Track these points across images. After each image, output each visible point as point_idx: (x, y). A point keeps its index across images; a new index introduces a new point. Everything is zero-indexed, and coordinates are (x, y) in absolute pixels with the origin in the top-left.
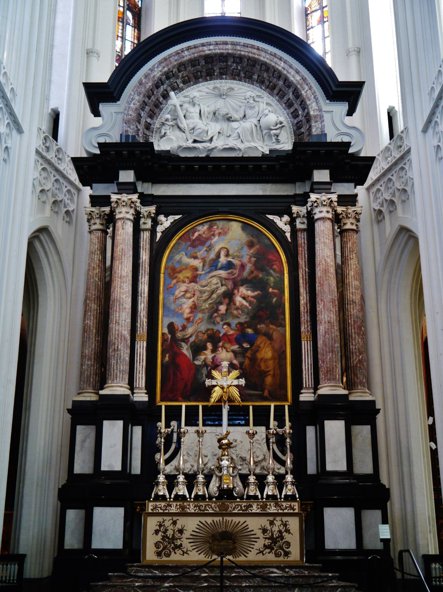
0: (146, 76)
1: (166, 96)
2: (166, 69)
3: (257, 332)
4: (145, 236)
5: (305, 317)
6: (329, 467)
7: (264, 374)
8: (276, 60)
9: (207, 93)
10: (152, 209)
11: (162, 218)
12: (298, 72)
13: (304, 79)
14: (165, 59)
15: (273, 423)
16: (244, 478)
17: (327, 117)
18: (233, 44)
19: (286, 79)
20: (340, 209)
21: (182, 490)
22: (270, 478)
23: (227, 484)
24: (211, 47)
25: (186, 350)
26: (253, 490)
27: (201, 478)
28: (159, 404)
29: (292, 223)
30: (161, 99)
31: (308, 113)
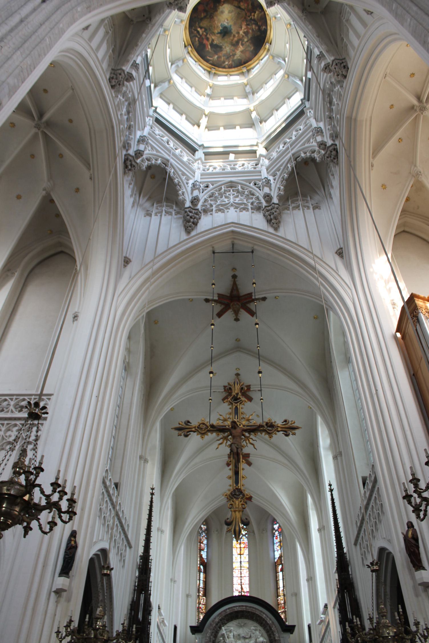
0: (213, 621)
1: (220, 628)
2: (220, 618)
8: (262, 613)
9: (236, 625)
12: (270, 619)
13: (273, 622)
14: (220, 613)
18: (246, 606)
19: (266, 622)
24: (237, 608)
30: (218, 629)
31: (275, 638)
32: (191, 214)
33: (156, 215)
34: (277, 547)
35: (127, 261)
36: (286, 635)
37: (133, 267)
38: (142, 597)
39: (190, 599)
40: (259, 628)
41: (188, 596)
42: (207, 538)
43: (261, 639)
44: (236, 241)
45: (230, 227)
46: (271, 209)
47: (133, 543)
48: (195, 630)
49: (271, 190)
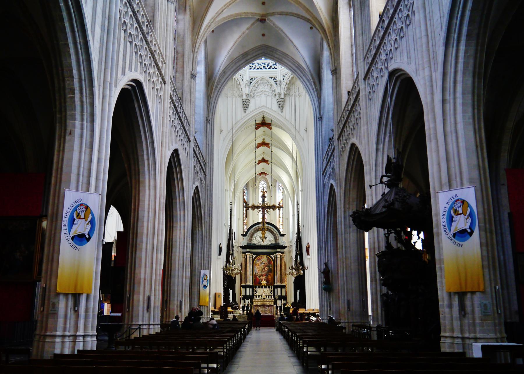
1: (254, 234)
3: (268, 274)
4: (251, 259)
5: (276, 272)
6: (278, 295)
7: (269, 281)
10: (252, 254)
11: (254, 255)
15: (271, 288)
16: (266, 296)
17: (280, 239)
20: (282, 254)
21: (258, 298)
22: (270, 296)
23: (264, 297)
25: (258, 277)
26: (268, 298)
27: (260, 296)
28: (254, 285)
29: (274, 256)
32: (246, 103)
33: (230, 97)
34: (281, 194)
35: (221, 131)
36: (282, 237)
37: (224, 133)
38: (231, 242)
39: (240, 220)
40: (270, 234)
41: (239, 219)
42: (247, 190)
43: (271, 239)
44: (264, 115)
45: (262, 109)
46: (280, 101)
47: (226, 225)
48: (243, 235)
49: (281, 87)
